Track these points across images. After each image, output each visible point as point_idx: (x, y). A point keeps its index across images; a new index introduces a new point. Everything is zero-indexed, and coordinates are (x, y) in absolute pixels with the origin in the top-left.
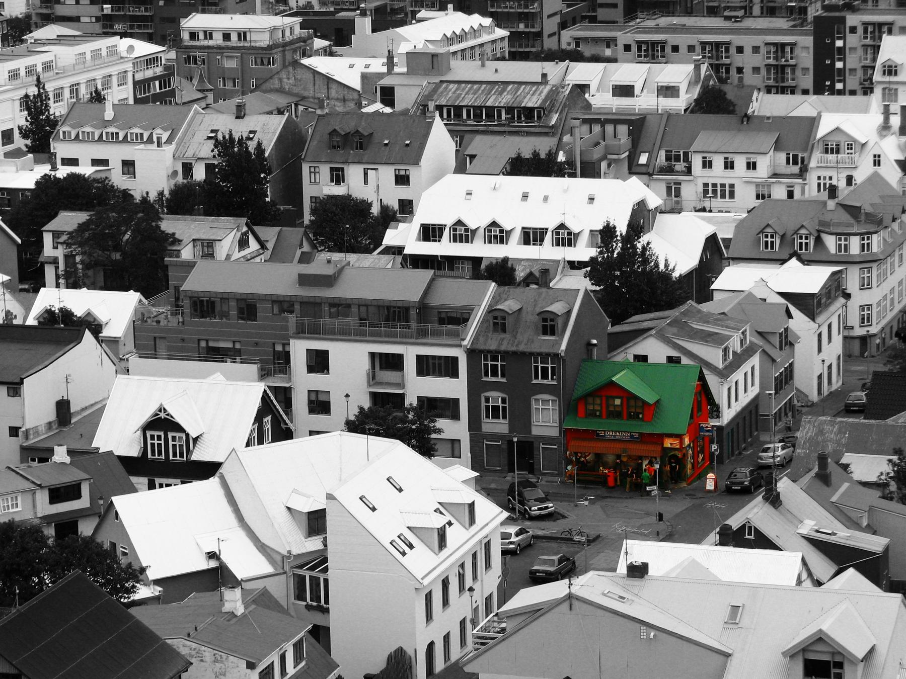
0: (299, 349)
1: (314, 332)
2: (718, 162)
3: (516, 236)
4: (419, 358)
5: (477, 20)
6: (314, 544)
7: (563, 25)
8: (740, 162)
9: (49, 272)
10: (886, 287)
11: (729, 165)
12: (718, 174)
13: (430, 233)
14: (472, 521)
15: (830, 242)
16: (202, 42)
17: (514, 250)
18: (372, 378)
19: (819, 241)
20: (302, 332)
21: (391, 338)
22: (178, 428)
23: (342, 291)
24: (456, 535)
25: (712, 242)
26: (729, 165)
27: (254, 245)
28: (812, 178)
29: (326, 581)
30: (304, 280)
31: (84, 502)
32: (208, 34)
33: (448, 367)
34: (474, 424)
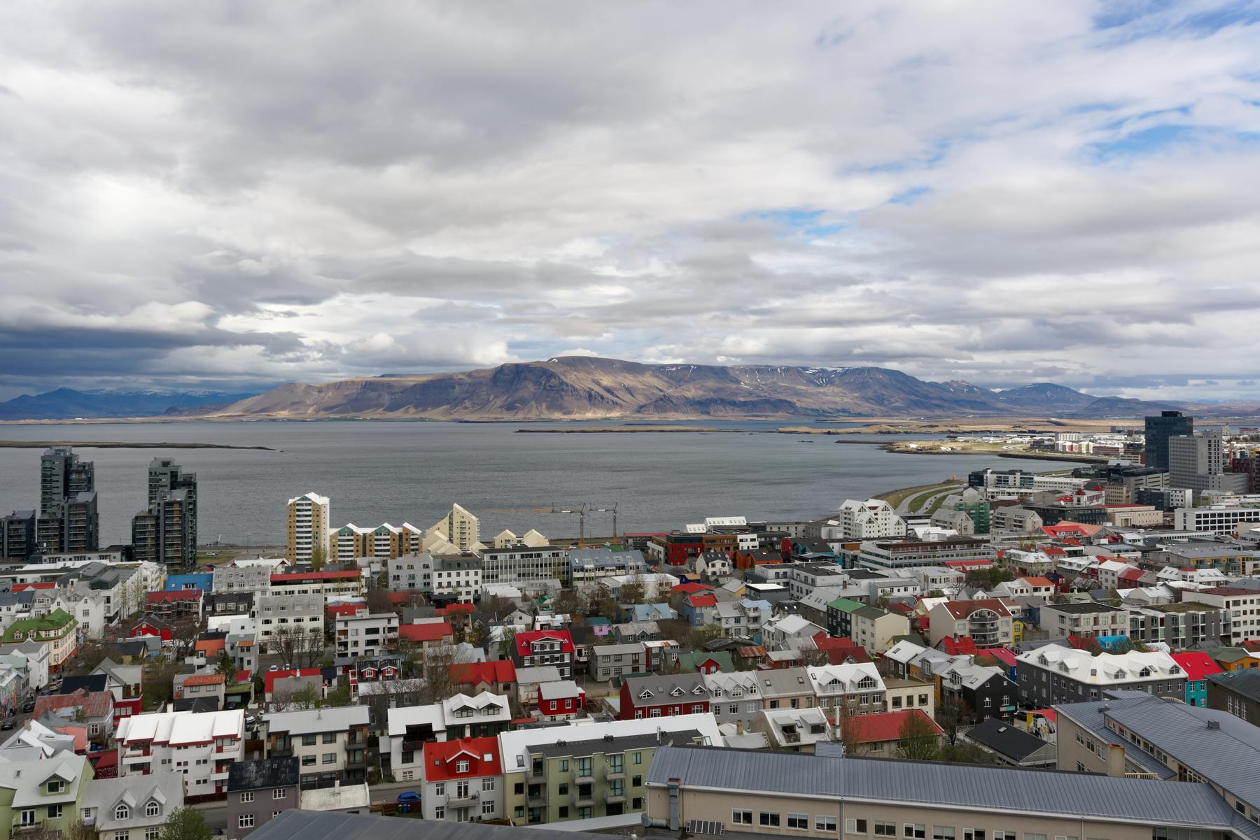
10: (64, 647)
15: (43, 634)
19: (38, 633)
28: (33, 612)
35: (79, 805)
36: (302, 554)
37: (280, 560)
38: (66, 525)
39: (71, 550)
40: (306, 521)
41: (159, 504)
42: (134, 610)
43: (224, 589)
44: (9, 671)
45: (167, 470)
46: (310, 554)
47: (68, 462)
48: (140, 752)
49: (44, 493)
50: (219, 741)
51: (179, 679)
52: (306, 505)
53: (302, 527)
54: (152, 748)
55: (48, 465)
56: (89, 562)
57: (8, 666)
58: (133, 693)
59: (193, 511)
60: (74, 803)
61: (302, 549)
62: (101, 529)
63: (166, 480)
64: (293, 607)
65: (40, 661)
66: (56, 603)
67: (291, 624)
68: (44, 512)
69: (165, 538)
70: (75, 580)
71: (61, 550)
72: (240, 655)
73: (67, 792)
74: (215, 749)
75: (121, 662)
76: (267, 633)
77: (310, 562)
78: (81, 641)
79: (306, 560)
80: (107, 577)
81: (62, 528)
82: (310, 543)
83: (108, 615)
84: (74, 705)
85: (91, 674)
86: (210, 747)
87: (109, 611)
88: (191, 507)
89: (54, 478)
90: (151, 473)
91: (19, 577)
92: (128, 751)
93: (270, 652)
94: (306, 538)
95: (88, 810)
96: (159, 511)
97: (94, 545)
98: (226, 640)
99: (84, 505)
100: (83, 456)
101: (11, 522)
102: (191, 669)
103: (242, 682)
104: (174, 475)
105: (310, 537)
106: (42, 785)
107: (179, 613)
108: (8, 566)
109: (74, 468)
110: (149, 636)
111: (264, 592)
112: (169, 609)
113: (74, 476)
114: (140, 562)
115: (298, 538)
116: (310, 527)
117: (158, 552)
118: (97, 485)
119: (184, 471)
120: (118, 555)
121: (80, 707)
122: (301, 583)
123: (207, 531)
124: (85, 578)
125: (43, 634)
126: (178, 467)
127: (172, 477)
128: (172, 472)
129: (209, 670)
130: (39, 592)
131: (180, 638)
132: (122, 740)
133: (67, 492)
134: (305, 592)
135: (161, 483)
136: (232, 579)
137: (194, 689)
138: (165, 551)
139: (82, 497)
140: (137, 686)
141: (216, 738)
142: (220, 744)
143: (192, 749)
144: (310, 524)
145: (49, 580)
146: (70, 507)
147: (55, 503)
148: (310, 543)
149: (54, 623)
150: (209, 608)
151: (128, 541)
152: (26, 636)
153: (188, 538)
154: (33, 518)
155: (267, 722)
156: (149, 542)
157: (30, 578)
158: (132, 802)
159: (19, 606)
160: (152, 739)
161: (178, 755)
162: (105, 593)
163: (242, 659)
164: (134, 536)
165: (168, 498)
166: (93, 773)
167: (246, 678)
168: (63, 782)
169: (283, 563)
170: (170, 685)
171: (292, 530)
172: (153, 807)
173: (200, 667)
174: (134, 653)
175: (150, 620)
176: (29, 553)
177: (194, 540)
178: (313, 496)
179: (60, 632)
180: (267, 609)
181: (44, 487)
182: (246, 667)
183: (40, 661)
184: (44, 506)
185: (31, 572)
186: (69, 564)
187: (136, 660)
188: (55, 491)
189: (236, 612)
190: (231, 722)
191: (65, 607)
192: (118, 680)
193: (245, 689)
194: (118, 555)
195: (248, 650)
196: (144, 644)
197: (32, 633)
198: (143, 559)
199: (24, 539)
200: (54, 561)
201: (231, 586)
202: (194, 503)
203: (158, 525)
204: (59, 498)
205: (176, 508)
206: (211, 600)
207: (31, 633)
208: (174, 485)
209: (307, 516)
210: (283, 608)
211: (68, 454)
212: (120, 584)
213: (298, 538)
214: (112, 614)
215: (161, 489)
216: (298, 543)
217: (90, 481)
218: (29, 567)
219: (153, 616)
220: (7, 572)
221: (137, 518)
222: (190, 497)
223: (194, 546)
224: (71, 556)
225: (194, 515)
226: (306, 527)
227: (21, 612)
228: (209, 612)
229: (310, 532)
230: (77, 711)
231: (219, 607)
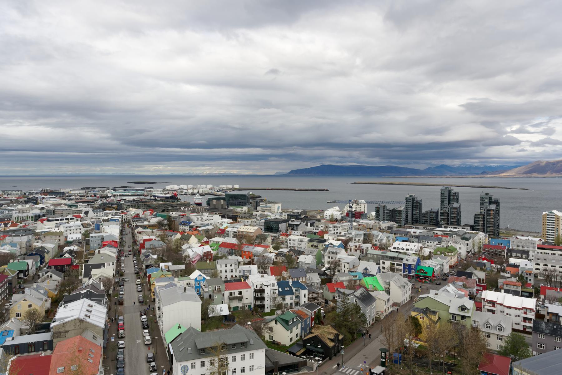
0: (381, 261)
1: (383, 259)
2: (429, 242)
3: (405, 250)
4: (397, 264)
5: (394, 223)
6: (388, 286)
7: (405, 224)
8: (432, 242)
9: (348, 249)
11: (431, 243)
12: (429, 244)
13: (395, 248)
14: (408, 285)
15: (447, 253)
16: (362, 224)
17: (405, 251)
18: (391, 266)
20: (382, 259)
21: (393, 261)
22: (368, 270)
23: (386, 255)
24: (406, 286)
25: (430, 252)
26: (431, 243)
27: (373, 248)
28: (442, 245)
29: (390, 291)
30: (382, 253)
31: (357, 278)
32: (363, 223)
33: (400, 265)
34: (404, 272)
35: (473, 319)
36: (549, 237)
37: (539, 239)
38: (449, 215)
39: (451, 224)
40: (551, 223)
41: (484, 210)
42: (476, 250)
43: (515, 248)
44: (438, 264)
45: (488, 197)
46: (554, 238)
47: (450, 192)
48: (492, 305)
49: (442, 203)
50: (525, 310)
51: (500, 281)
52: (552, 215)
53: (549, 225)
54: (496, 305)
55: (443, 192)
56: (459, 230)
57: (437, 263)
58: (482, 282)
59: (498, 214)
60: (470, 317)
61: (550, 235)
62: (462, 218)
63: (487, 201)
64: (551, 260)
65: (447, 263)
66: (449, 243)
67: (549, 267)
68: (441, 210)
69: (487, 224)
70: (455, 236)
71: (448, 224)
72: (527, 276)
73: (468, 313)
74: (523, 312)
75: (476, 269)
76: (537, 269)
77: (554, 241)
78: (459, 259)
79: (551, 240)
80: (467, 236)
81: (448, 216)
82: (554, 233)
83: (468, 250)
84: (462, 281)
85: (466, 271)
86: (521, 311)
87: (468, 249)
88: (498, 212)
89: (445, 197)
90: (481, 197)
91: (436, 232)
92: (487, 304)
93: (539, 277)
94: (552, 230)
95: (475, 321)
96: (484, 213)
97: (459, 223)
98: (520, 269)
99: (456, 208)
100: (455, 190)
101: (431, 212)
102: (504, 277)
103: (528, 288)
104: (490, 198)
105: (554, 230)
106: (459, 307)
107: (496, 254)
108: (431, 228)
109: (452, 194)
110: (485, 261)
111: (534, 251)
112: (492, 252)
113: (452, 197)
114: (478, 232)
115: (547, 230)
116: (554, 225)
117: (484, 229)
118: (460, 201)
119: (494, 197)
120: (469, 228)
121: (465, 283)
122: (553, 250)
123: (504, 222)
124: (459, 235)
125: (447, 253)
126: (492, 195)
127: (489, 200)
128: (489, 198)
129: (514, 280)
130: (444, 238)
131: (498, 264)
132: (484, 299)
133: (449, 203)
134: (555, 254)
135: (485, 202)
136: (519, 244)
137: (508, 286)
138: (487, 229)
139: (455, 205)
140: (483, 280)
141: (523, 308)
142: (525, 311)
143: (513, 310)
144: (554, 224)
145: (446, 234)
146: (451, 208)
147: (445, 207)
148: (554, 233)
149: (451, 250)
150: (509, 254)
151: (472, 223)
152: (441, 253)
153: (496, 225)
154: (438, 212)
155: (547, 307)
156: (480, 225)
157: (439, 233)
158: (492, 323)
159: (436, 242)
160: (496, 302)
161: (507, 311)
162: (467, 242)
163: (527, 278)
164: (474, 222)
165: (488, 208)
166: (475, 308)
167: (530, 286)
168: (466, 309)
169: (540, 240)
170: (497, 282)
171: (545, 226)
172: (500, 328)
173: (508, 278)
174: (482, 267)
175: (485, 255)
176: (437, 224)
177: (499, 225)
178: (555, 212)
179: (453, 254)
180: (538, 259)
181: (441, 201)
182: (529, 282)
183: (447, 263)
184: (441, 208)
185: (440, 231)
186: (452, 229)
187: (482, 270)
188: (445, 202)
189: (522, 258)
190: (530, 303)
191: (453, 244)
192: (476, 276)
193: (531, 291)
194: (469, 228)
195: (530, 274)
196: (485, 264)
197: (443, 252)
198: (479, 231)
199: (435, 219)
200: (446, 227)
201: (518, 246)
202: (499, 211)
203: (484, 218)
204: (446, 205)
205: (492, 212)
206: (510, 251)
207: (443, 252)
208: (490, 203)
209: (552, 220)
210: (545, 260)
211: (450, 189)
212: (472, 239)
213: (547, 230)
214: (469, 251)
215: (485, 204)
216: (547, 232)
217: (457, 199)
218: (438, 229)
219: (486, 253)
220: (430, 230)
221: (476, 215)
222: (497, 208)
223: (499, 228)
224: (452, 227)
225: (499, 216)
226: (552, 225)
227: (438, 244)
228: (509, 256)
229: (554, 228)
230: (464, 284)
231: (514, 255)
